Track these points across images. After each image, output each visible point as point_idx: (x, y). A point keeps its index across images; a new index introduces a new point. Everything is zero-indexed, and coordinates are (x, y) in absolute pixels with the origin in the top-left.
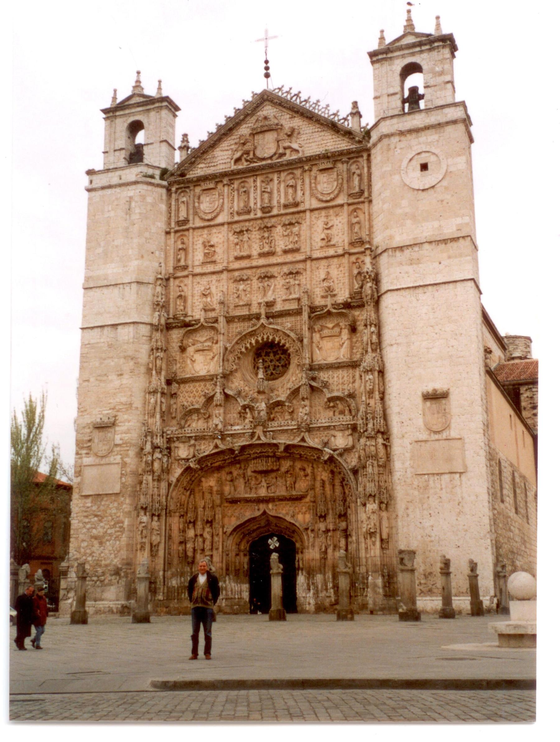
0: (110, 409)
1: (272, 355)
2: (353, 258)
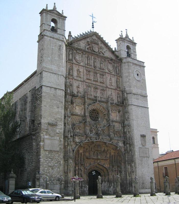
0: (54, 119)
1: (94, 113)
2: (118, 91)
